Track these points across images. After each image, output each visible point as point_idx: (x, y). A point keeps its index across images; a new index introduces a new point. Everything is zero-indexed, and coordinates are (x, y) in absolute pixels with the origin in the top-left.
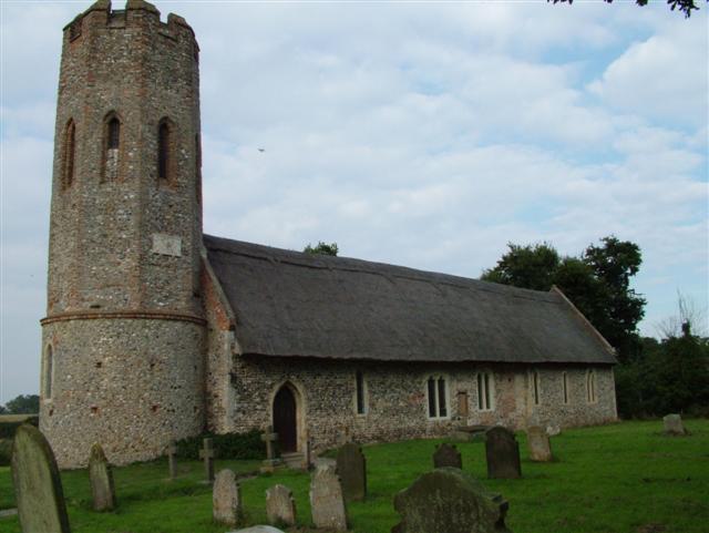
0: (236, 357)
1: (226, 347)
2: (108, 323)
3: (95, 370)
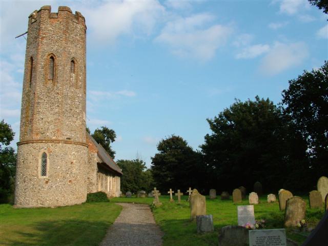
1: (95, 159)
2: (75, 146)
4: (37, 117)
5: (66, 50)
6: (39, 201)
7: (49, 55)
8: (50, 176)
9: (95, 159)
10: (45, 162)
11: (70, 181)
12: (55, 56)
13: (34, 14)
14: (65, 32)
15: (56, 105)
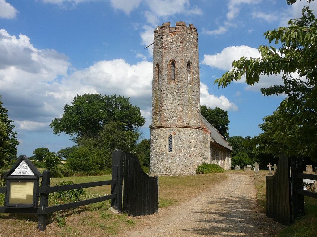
0: (211, 143)
1: (208, 139)
2: (193, 129)
3: (189, 144)
4: (165, 108)
5: (183, 56)
6: (167, 170)
7: (171, 61)
8: (175, 152)
9: (208, 139)
10: (171, 142)
11: (190, 156)
12: (175, 62)
13: (158, 29)
14: (182, 42)
15: (178, 99)
